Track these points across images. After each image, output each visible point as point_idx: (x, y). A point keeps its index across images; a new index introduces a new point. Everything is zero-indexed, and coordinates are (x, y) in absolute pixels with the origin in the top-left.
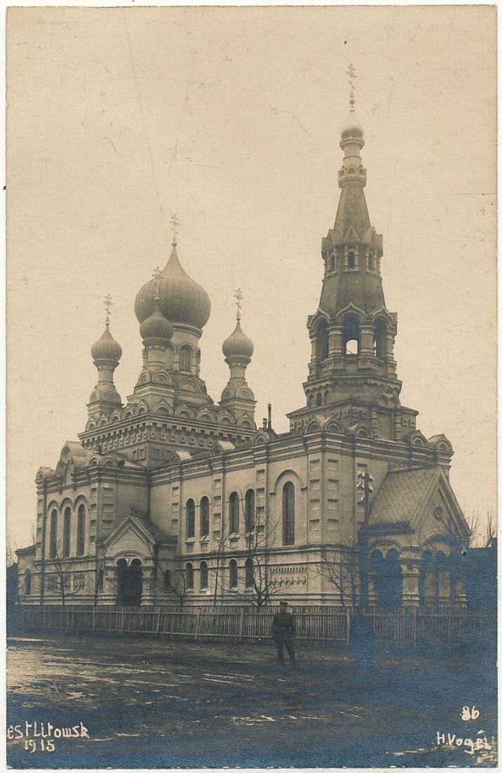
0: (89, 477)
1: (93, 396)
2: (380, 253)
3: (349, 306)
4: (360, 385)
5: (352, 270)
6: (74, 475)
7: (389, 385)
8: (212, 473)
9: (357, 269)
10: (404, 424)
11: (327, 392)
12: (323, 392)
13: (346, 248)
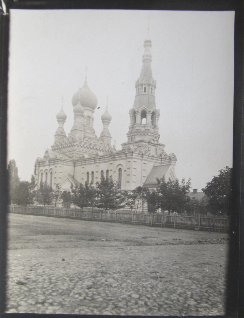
4: (146, 135)
5: (145, 93)
9: (146, 93)
10: (160, 149)
11: (134, 137)
12: (133, 137)
13: (143, 85)
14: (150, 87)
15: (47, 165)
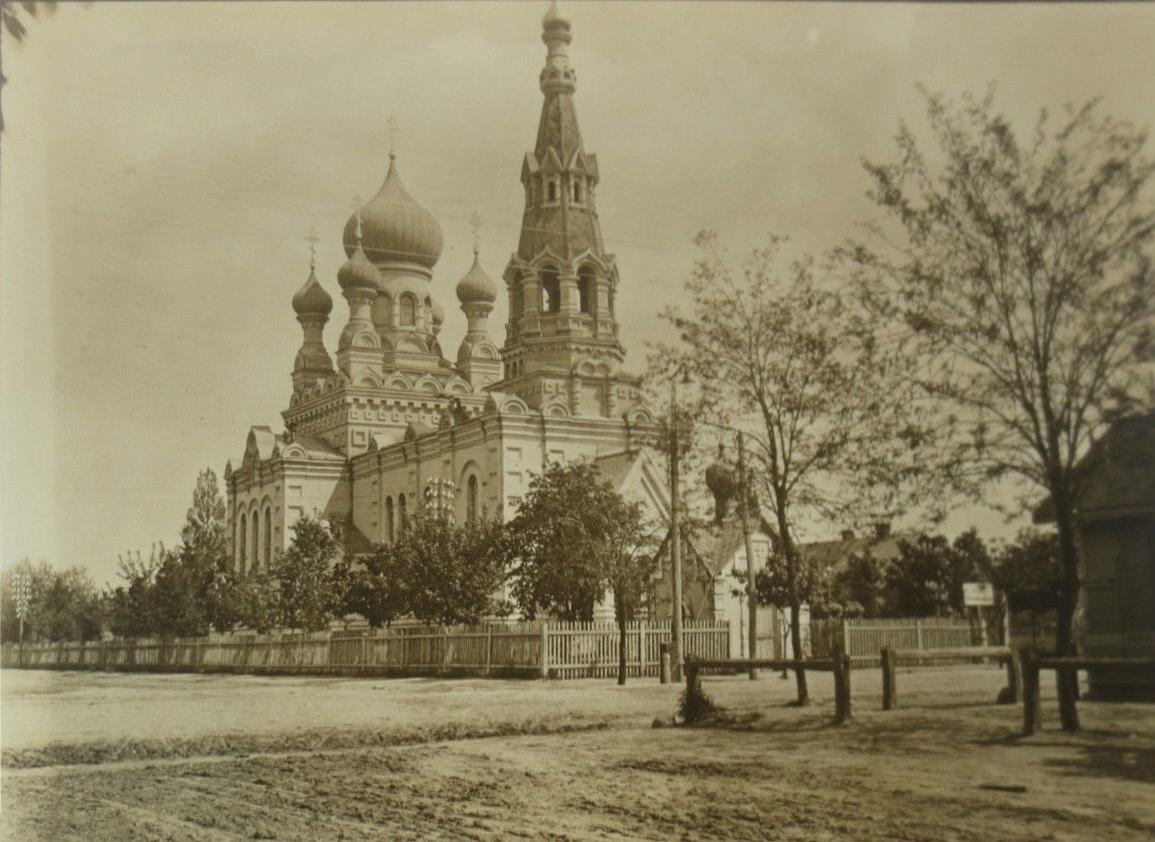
0: (273, 472)
1: (297, 361)
2: (592, 179)
3: (543, 253)
6: (261, 469)
7: (596, 348)
8: (407, 462)
14: (568, 180)
15: (254, 484)
